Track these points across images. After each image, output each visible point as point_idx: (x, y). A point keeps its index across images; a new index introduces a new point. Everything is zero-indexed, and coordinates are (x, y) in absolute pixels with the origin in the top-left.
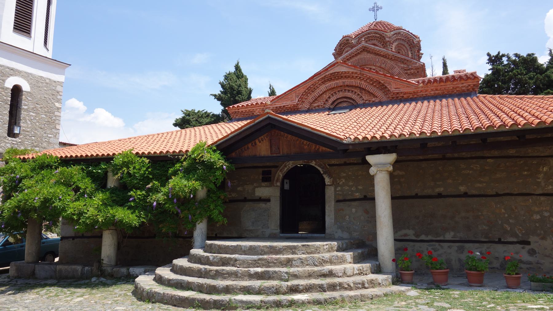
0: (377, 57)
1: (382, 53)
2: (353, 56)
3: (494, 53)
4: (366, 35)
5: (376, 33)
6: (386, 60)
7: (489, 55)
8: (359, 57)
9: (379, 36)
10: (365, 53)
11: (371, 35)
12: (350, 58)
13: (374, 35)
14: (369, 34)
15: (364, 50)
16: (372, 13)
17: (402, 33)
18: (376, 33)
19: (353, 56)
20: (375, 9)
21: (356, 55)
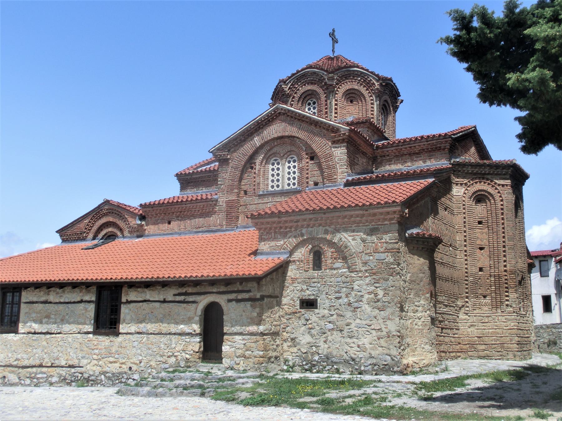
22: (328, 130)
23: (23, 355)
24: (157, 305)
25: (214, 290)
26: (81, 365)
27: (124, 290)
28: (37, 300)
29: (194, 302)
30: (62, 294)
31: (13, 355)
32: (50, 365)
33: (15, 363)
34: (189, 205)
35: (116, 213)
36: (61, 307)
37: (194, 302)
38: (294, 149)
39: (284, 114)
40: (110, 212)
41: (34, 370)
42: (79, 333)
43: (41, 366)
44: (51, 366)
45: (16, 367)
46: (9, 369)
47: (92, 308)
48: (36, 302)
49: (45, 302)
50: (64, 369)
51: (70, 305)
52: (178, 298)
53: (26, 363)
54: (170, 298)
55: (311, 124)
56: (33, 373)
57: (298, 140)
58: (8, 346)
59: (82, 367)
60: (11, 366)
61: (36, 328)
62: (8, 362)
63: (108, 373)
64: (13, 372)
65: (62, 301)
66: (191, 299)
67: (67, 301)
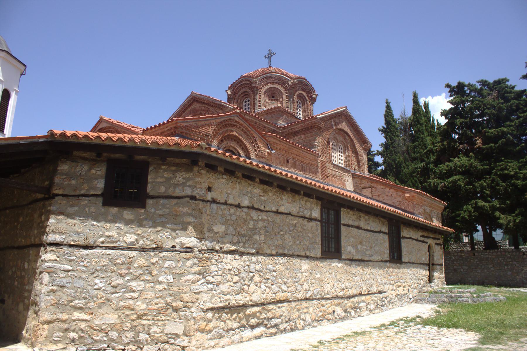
0: (204, 105)
1: (205, 102)
2: (187, 108)
3: (454, 84)
4: (239, 83)
5: (246, 80)
6: (209, 108)
7: (448, 86)
8: (192, 107)
9: (249, 82)
10: (195, 103)
11: (244, 83)
12: (185, 110)
13: (245, 82)
14: (241, 82)
15: (194, 100)
16: (267, 60)
17: (274, 76)
18: (246, 80)
19: (187, 108)
20: (270, 55)
21: (188, 106)
22: (361, 140)
23: (347, 284)
24: (415, 241)
25: (432, 236)
26: (385, 291)
27: (402, 227)
28: (352, 224)
29: (427, 243)
30: (369, 222)
31: (338, 284)
32: (366, 293)
33: (341, 294)
34: (304, 153)
35: (242, 130)
36: (369, 234)
37: (427, 243)
38: (343, 141)
39: (345, 116)
40: (236, 126)
41: (356, 299)
42: (382, 261)
43: (361, 295)
44: (368, 294)
45: (342, 298)
46: (336, 301)
47: (386, 238)
48: (351, 226)
49: (358, 228)
50: (376, 295)
51: (375, 234)
52: (422, 239)
53: (351, 292)
54: (419, 238)
55: (355, 131)
56: (357, 302)
57: (347, 137)
58: (334, 273)
59: (385, 292)
60: (337, 297)
61: (354, 254)
62: (335, 293)
63: (399, 295)
64: (338, 305)
65: (369, 229)
66: (426, 240)
67: (372, 229)
